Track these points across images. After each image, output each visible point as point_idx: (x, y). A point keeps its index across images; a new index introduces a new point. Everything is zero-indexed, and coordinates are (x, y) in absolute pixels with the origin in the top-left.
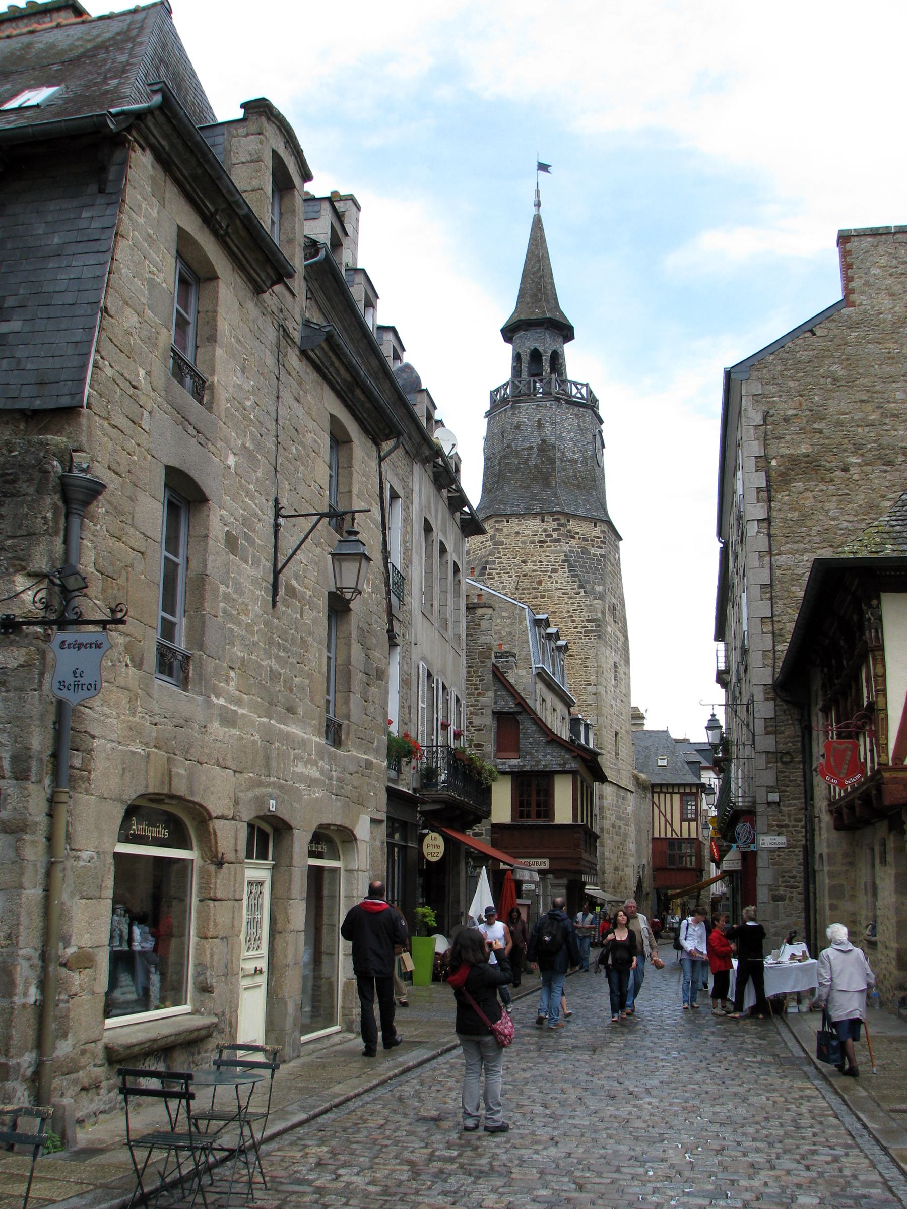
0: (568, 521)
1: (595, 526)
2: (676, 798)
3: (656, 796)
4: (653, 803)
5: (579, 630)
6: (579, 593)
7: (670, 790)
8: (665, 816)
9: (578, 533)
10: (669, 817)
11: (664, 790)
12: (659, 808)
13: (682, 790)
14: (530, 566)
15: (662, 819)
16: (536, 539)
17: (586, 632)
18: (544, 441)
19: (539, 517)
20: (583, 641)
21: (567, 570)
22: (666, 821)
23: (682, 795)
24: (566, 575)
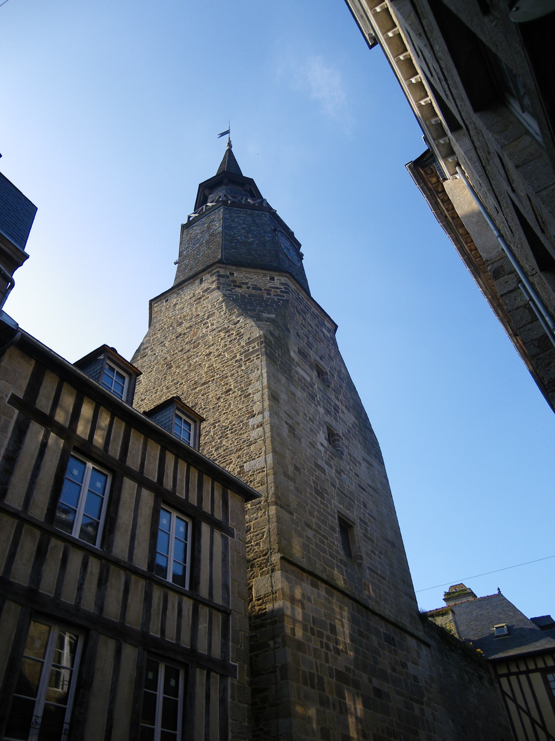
0: (232, 274)
1: (272, 279)
2: (536, 678)
3: (504, 681)
4: (504, 693)
5: (238, 358)
6: (239, 321)
7: (523, 668)
8: (528, 714)
9: (247, 283)
10: (534, 713)
11: (514, 669)
12: (514, 700)
13: (541, 665)
14: (186, 324)
15: (526, 719)
16: (194, 299)
17: (246, 356)
18: (212, 235)
19: (198, 281)
20: (243, 368)
21: (224, 308)
22: (533, 721)
23: (544, 672)
24: (222, 313)
